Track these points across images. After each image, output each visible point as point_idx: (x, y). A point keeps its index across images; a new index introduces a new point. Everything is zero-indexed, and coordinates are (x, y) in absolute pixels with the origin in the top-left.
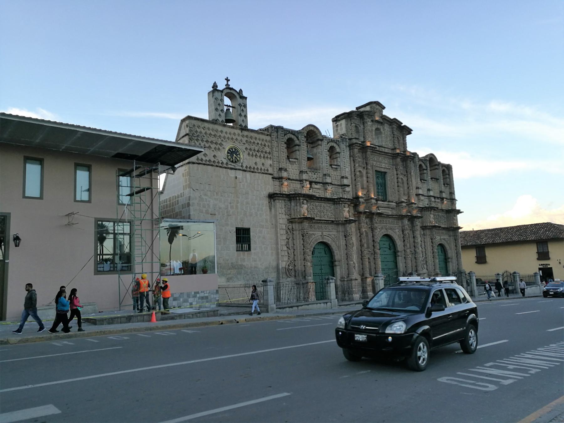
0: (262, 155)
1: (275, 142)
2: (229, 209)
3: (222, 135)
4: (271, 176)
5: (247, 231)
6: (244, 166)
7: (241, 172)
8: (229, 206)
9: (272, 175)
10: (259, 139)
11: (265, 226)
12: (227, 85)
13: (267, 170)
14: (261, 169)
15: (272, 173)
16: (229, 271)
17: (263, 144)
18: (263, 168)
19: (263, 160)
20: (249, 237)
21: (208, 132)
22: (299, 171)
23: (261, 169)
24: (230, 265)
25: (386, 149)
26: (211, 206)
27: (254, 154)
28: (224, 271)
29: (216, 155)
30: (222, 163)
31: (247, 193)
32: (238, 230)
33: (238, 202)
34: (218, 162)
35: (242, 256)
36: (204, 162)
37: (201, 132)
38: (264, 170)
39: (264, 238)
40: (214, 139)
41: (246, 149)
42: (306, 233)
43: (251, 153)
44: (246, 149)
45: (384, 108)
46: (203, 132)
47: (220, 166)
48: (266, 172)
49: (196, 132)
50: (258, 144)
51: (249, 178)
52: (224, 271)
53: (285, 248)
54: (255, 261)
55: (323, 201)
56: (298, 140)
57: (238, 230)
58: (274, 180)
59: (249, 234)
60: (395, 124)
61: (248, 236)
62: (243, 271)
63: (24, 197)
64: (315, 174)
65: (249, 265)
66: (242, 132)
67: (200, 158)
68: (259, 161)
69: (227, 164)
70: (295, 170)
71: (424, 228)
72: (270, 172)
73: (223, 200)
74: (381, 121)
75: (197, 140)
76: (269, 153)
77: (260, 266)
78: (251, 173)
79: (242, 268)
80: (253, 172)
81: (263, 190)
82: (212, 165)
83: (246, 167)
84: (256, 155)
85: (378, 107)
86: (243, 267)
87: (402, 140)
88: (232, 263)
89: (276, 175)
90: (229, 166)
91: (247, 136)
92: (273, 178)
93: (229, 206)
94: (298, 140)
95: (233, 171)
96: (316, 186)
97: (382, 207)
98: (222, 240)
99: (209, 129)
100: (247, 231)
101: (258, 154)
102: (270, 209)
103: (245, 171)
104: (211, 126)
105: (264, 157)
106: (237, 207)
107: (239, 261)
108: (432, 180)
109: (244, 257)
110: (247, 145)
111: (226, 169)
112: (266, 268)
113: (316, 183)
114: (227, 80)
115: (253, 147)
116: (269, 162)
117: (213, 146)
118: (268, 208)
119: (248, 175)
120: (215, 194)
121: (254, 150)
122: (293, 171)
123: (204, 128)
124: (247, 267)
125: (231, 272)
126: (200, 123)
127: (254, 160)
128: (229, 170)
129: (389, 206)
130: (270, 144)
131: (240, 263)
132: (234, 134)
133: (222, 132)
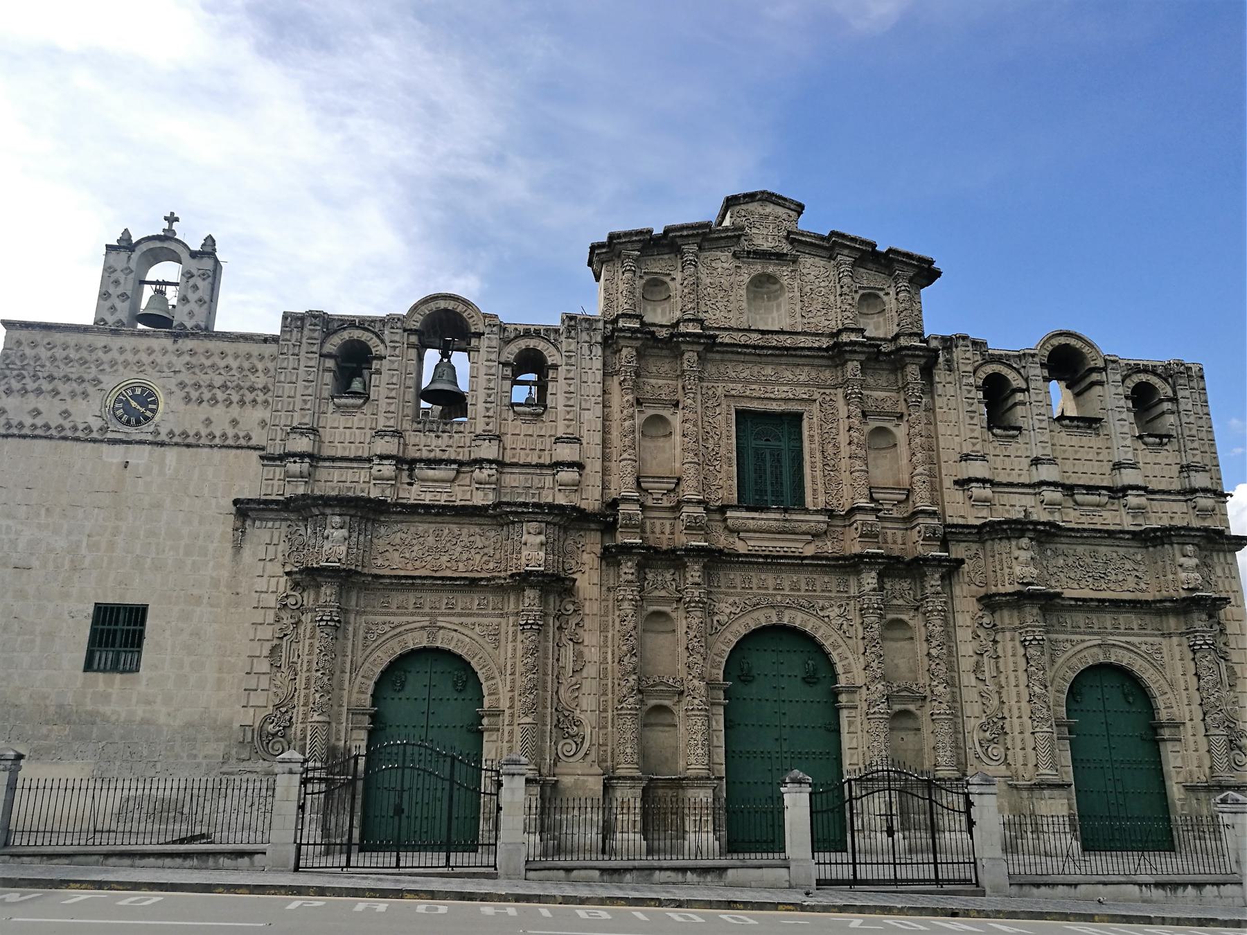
1: (291, 357)
2: (84, 551)
5: (138, 614)
6: (164, 431)
7: (147, 448)
8: (84, 544)
9: (263, 449)
11: (205, 601)
14: (224, 435)
16: (44, 730)
17: (246, 365)
18: (230, 433)
19: (235, 411)
20: (142, 633)
23: (224, 435)
24: (52, 710)
26: (21, 545)
27: (207, 395)
28: (28, 727)
29: (71, 410)
30: (88, 429)
31: (158, 505)
32: (104, 613)
33: (116, 532)
34: (75, 429)
35: (101, 687)
36: (26, 431)
37: (37, 358)
38: (237, 437)
39: (196, 634)
40: (74, 371)
42: (329, 618)
43: (194, 395)
44: (182, 385)
46: (44, 354)
47: (86, 437)
48: (243, 442)
49: (23, 357)
51: (174, 463)
52: (28, 727)
53: (264, 666)
54: (148, 703)
55: (433, 519)
56: (383, 341)
57: (104, 613)
58: (266, 462)
59: (143, 623)
60: (846, 252)
61: (138, 628)
62: (95, 730)
64: (438, 437)
65: (123, 715)
66: (175, 342)
67: (14, 423)
68: (220, 417)
69: (103, 430)
70: (357, 431)
71: (990, 602)
72: (253, 443)
73: (65, 526)
74: (786, 248)
76: (265, 389)
77: (162, 719)
78: (184, 449)
79: (93, 723)
80: (188, 446)
81: (219, 494)
82: (50, 438)
83: (171, 433)
84: (214, 398)
85: (770, 208)
86: (98, 720)
87: (894, 301)
88: (61, 706)
90: (109, 435)
92: (262, 458)
93: (84, 544)
94: (383, 341)
95: (120, 448)
96: (431, 473)
97: (755, 531)
98: (38, 640)
100: (138, 614)
101: (220, 396)
102: (238, 548)
103: (162, 444)
104: (101, 340)
106: (111, 546)
107: (88, 700)
108: (1067, 426)
109: (110, 690)
110: (186, 377)
111: (96, 445)
112: (190, 725)
113: (431, 463)
115: (204, 379)
116: (260, 413)
117: (64, 388)
118: (229, 546)
119: (171, 455)
120: (43, 511)
121: (211, 386)
123: (50, 346)
124: (114, 718)
125: (50, 731)
126: (38, 335)
127: (204, 411)
128: (105, 447)
129: (787, 525)
131: (89, 708)
133: (106, 349)
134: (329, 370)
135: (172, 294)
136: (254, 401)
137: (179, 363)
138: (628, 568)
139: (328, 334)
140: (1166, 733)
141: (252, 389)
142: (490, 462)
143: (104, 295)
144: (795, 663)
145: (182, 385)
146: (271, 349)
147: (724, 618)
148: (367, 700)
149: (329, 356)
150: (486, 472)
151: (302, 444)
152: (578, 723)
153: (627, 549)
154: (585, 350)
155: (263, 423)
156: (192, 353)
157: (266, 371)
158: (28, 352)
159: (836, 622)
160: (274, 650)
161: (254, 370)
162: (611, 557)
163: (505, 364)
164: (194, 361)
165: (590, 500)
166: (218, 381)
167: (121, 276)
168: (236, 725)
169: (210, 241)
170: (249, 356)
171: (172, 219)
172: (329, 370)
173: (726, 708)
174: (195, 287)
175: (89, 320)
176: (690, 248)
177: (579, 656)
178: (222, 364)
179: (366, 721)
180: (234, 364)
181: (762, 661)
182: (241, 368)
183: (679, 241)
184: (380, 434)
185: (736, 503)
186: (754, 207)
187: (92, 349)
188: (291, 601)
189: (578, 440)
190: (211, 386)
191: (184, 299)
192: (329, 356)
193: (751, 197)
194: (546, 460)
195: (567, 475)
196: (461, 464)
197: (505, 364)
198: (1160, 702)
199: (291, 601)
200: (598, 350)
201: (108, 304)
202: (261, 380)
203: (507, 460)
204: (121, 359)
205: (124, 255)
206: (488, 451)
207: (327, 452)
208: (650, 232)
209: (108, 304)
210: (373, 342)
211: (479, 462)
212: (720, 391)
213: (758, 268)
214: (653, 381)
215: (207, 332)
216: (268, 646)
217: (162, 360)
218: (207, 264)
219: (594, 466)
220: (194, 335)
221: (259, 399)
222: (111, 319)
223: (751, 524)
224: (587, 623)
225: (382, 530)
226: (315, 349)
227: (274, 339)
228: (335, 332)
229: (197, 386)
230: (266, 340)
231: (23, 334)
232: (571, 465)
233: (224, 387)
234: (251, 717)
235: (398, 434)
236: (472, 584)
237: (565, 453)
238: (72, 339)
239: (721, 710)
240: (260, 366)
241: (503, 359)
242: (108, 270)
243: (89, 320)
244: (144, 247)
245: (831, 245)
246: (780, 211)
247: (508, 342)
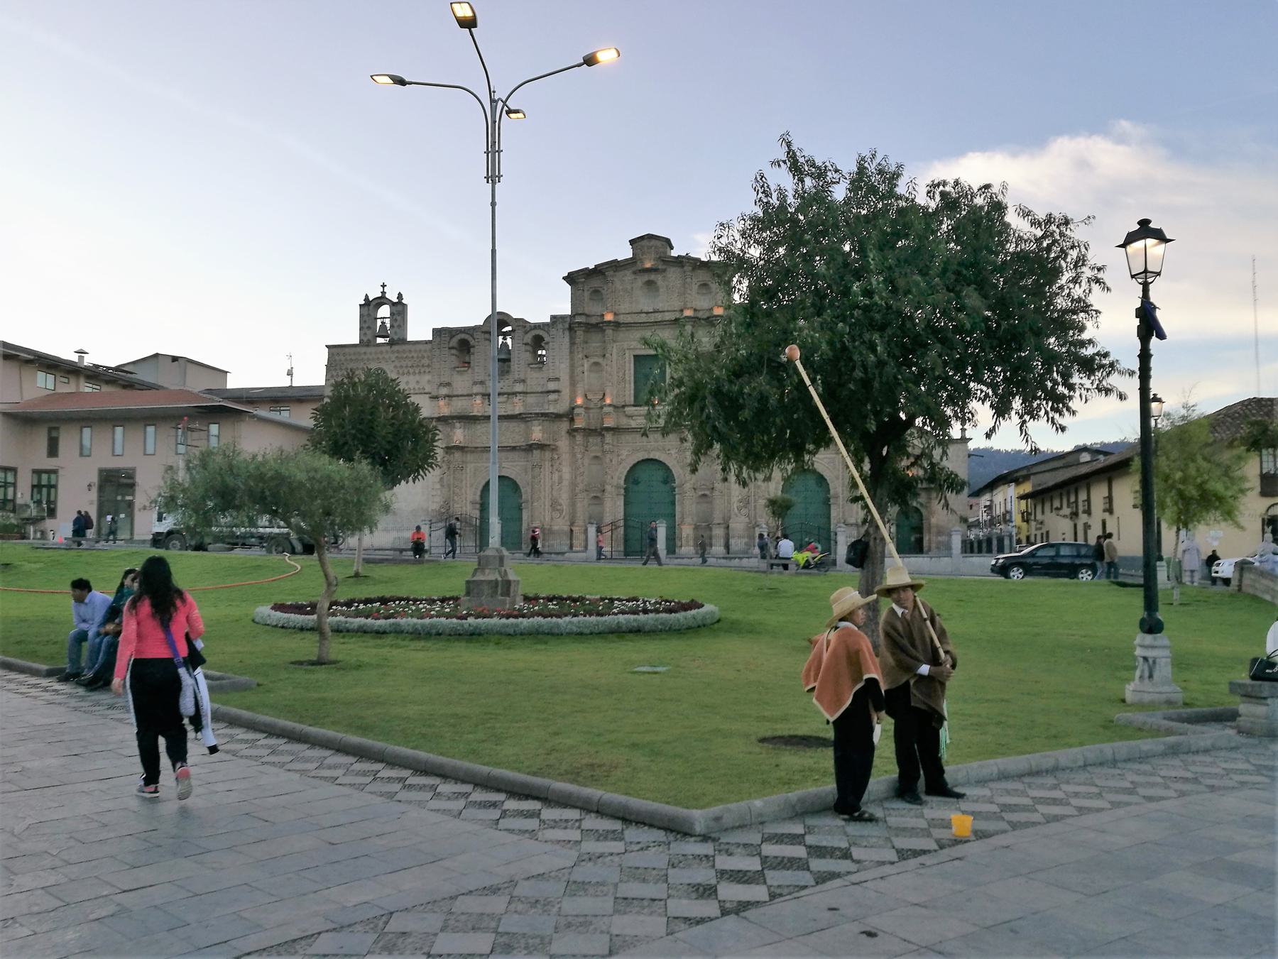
0: (417, 372)
3: (365, 357)
4: (428, 395)
10: (415, 351)
12: (383, 293)
13: (424, 389)
15: (430, 391)
18: (417, 387)
19: (417, 377)
21: (349, 358)
22: (471, 382)
25: (666, 314)
27: (406, 371)
37: (340, 360)
38: (419, 389)
41: (395, 367)
45: (668, 241)
46: (343, 358)
49: (335, 360)
50: (413, 357)
53: (438, 486)
63: (145, 454)
72: (426, 391)
75: (336, 369)
76: (428, 366)
84: (408, 372)
85: (653, 242)
89: (434, 394)
91: (398, 352)
99: (354, 354)
101: (411, 371)
104: (363, 350)
105: (420, 373)
110: (397, 363)
114: (384, 286)
116: (427, 377)
122: (462, 383)
130: (429, 354)
132: (381, 353)
133: (365, 353)
134: (453, 355)
135: (388, 321)
136: (425, 372)
137: (393, 357)
138: (579, 438)
139: (452, 337)
140: (832, 501)
141: (423, 366)
142: (520, 393)
143: (361, 329)
144: (660, 475)
145: (395, 367)
146: (429, 346)
147: (623, 457)
148: (478, 498)
149: (453, 348)
150: (518, 398)
151: (444, 391)
152: (561, 505)
153: (577, 430)
154: (561, 333)
155: (429, 381)
156: (398, 352)
157: (428, 357)
158: (337, 358)
159: (674, 456)
160: (441, 479)
161: (423, 357)
162: (572, 432)
163: (526, 344)
164: (400, 356)
165: (562, 407)
166: (410, 364)
167: (366, 318)
168: (430, 510)
169: (400, 297)
170: (420, 351)
171: (384, 286)
172: (453, 355)
173: (625, 496)
174: (396, 320)
175: (357, 342)
176: (609, 273)
177: (561, 478)
178: (410, 356)
179: (478, 506)
180: (415, 355)
181: (644, 475)
182: (418, 357)
183: (604, 271)
184: (475, 383)
185: (632, 403)
186: (645, 243)
187: (359, 354)
188: (446, 459)
189: (557, 379)
190: (407, 367)
191: (392, 326)
192: (453, 348)
193: (642, 238)
194: (544, 389)
195: (552, 397)
196: (508, 394)
197: (526, 344)
198: (831, 486)
199: (446, 459)
200: (567, 333)
201: (363, 332)
202: (426, 362)
203: (528, 391)
204: (371, 357)
205: (366, 308)
206: (519, 387)
207: (455, 393)
208: (587, 269)
209: (363, 332)
210: (470, 339)
211: (515, 394)
212: (625, 347)
213: (646, 277)
214: (594, 345)
215: (403, 341)
216: (438, 478)
217: (387, 356)
218: (399, 308)
219: (566, 392)
220: (398, 344)
221: (427, 371)
222: (365, 339)
223: (636, 413)
224: (563, 463)
225: (479, 427)
226: (446, 345)
227: (430, 342)
228: (454, 336)
229: (401, 367)
230: (427, 342)
231: (333, 350)
232: (554, 392)
233: (412, 366)
234: (435, 506)
235: (482, 383)
236: (514, 448)
237: (552, 386)
238: (353, 350)
239: (623, 497)
240: (425, 355)
241: (525, 342)
242: (361, 316)
243: (357, 342)
244: (374, 303)
245: (683, 261)
246: (658, 243)
247: (526, 333)
